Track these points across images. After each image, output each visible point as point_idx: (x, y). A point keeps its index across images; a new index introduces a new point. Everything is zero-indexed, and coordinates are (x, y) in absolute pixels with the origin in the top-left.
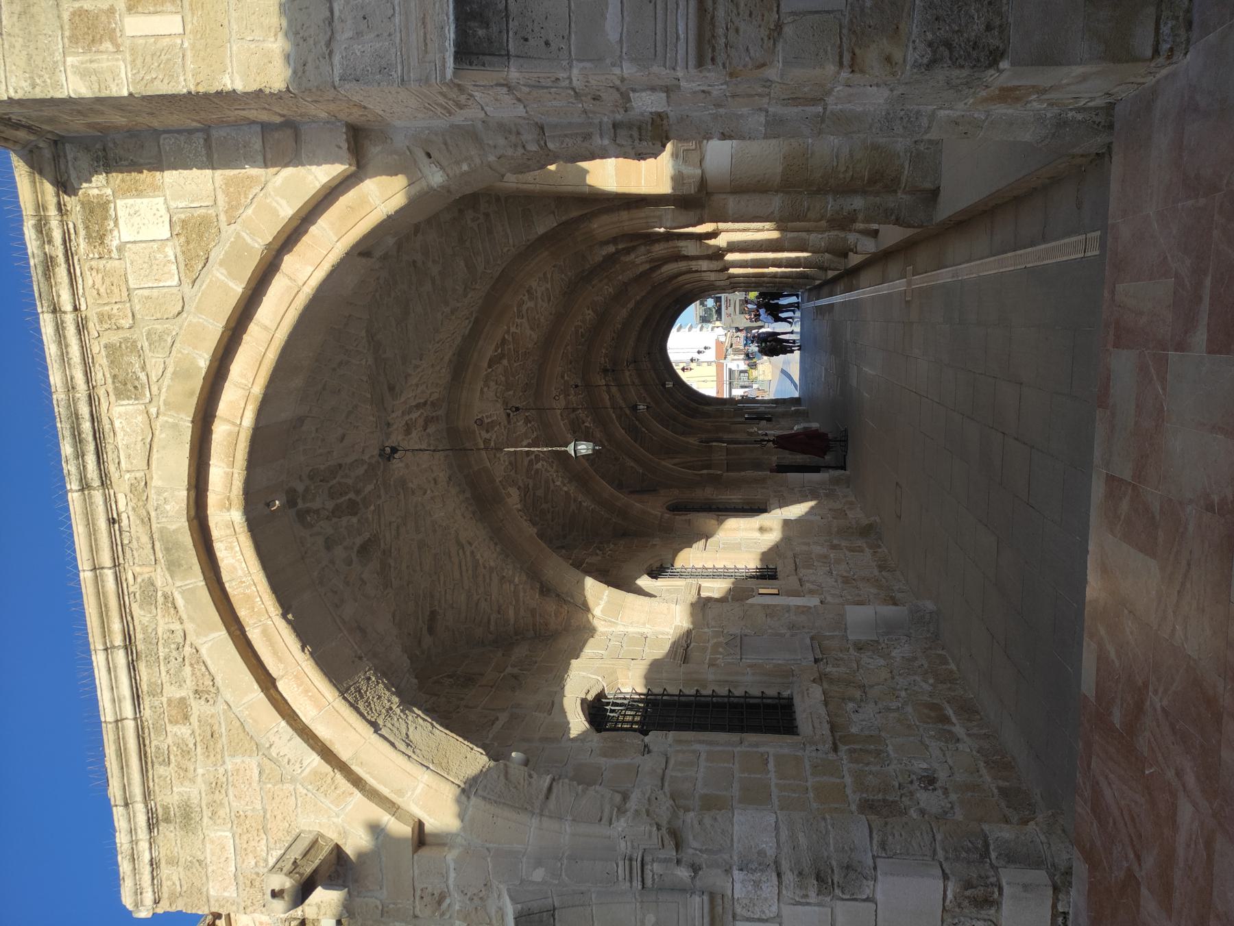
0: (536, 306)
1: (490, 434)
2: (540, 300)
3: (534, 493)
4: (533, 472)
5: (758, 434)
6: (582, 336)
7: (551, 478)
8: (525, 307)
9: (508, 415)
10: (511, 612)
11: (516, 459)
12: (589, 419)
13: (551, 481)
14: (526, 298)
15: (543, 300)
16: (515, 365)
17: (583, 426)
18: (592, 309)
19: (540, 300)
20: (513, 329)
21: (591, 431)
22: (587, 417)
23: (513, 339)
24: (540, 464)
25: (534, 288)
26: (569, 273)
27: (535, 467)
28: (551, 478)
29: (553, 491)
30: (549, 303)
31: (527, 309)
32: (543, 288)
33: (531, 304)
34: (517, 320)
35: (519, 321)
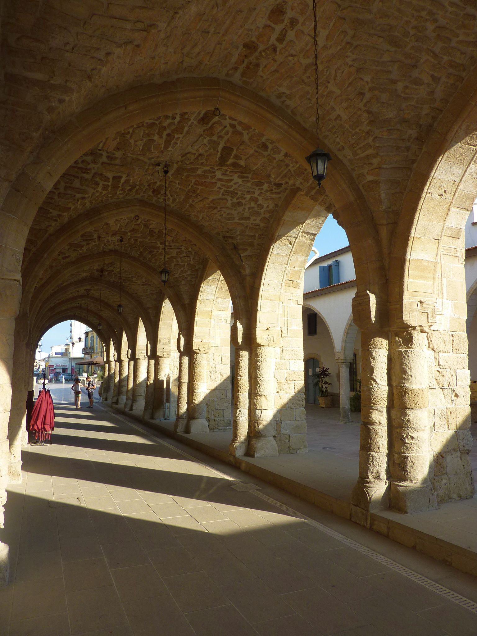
3: (77, 177)
4: (97, 179)
8: (229, 198)
9: (158, 165)
10: (38, 76)
11: (116, 165)
13: (84, 196)
14: (235, 200)
15: (228, 214)
16: (193, 181)
17: (84, 243)
19: (229, 211)
20: (219, 184)
21: (79, 249)
25: (239, 208)
26: (239, 238)
27: (101, 183)
28: (87, 196)
29: (75, 196)
30: (225, 218)
31: (227, 200)
33: (229, 204)
35: (222, 191)
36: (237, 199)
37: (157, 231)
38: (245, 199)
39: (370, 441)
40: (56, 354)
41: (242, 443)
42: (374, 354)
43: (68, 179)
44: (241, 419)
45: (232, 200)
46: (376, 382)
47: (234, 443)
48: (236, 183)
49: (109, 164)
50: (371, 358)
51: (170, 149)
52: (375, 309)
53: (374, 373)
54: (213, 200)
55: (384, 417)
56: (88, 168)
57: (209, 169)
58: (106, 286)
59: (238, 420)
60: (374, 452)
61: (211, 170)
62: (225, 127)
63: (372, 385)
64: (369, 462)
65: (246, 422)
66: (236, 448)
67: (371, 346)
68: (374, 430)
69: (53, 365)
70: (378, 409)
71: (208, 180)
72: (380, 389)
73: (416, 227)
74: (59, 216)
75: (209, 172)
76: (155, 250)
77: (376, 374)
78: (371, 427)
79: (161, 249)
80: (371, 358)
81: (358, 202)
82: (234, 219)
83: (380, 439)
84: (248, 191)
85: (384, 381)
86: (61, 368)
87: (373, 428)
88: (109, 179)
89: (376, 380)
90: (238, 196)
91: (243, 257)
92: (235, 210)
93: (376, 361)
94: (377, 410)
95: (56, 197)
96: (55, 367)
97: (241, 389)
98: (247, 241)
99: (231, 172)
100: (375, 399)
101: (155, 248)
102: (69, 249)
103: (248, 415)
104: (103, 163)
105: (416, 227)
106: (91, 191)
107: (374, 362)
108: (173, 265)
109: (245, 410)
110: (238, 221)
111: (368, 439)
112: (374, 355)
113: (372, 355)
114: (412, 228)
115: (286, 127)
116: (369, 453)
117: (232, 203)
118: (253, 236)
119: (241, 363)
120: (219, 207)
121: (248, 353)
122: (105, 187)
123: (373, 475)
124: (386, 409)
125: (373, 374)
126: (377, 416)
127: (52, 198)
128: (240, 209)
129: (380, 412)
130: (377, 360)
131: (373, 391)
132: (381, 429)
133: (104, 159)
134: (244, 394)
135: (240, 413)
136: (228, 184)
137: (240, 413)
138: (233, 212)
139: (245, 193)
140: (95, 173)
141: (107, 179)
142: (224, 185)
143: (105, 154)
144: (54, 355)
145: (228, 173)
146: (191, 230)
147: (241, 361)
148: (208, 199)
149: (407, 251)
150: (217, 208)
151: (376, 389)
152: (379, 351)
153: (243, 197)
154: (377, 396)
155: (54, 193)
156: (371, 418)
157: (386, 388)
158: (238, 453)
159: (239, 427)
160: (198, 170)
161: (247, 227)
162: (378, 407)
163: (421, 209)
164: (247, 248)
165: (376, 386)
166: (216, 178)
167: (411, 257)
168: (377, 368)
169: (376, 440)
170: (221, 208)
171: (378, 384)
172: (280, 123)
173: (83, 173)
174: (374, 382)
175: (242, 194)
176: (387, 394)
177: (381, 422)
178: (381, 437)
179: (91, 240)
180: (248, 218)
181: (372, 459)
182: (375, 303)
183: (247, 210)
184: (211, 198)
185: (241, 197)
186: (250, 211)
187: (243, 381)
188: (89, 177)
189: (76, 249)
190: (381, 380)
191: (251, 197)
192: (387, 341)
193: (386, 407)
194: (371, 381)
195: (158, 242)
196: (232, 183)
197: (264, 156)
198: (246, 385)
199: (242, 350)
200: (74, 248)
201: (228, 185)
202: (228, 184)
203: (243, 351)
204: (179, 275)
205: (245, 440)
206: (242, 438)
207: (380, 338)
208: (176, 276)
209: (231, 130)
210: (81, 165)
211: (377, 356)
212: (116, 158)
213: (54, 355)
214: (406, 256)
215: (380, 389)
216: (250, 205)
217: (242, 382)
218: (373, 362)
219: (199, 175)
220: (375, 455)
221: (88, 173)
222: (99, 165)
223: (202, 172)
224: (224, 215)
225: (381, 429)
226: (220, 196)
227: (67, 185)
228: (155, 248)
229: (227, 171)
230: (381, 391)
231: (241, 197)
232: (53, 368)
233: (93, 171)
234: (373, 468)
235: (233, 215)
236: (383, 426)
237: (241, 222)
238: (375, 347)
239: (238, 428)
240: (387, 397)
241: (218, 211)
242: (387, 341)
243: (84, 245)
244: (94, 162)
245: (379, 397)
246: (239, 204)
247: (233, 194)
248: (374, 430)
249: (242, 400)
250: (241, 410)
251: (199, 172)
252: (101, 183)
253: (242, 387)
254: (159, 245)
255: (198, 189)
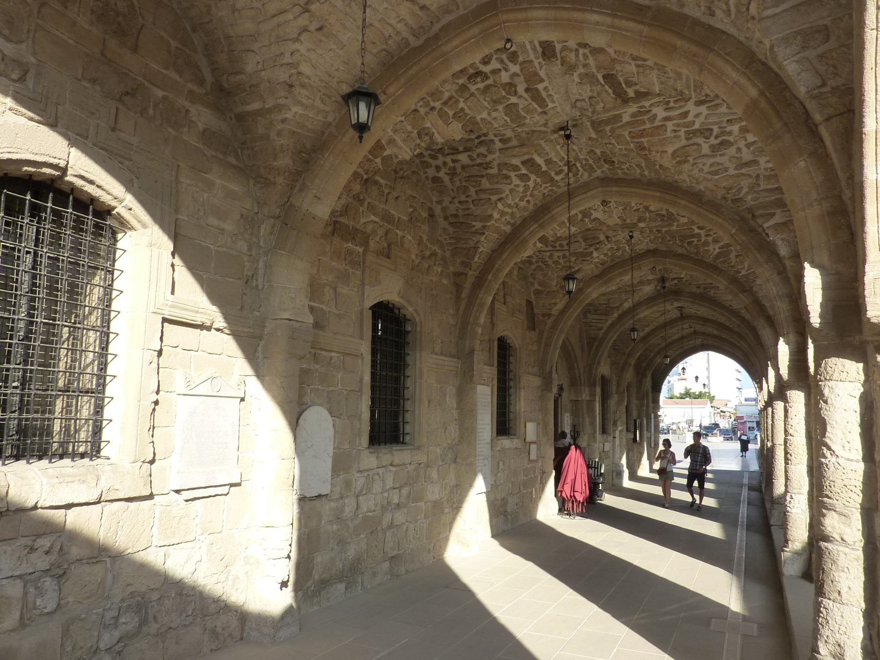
0: (703, 156)
1: (525, 95)
2: (712, 160)
3: (482, 176)
4: (505, 172)
5: (614, 431)
6: (690, 243)
7: (503, 195)
8: (700, 140)
12: (602, 257)
14: (713, 141)
15: (711, 165)
16: (626, 133)
17: (592, 249)
18: (719, 253)
19: (712, 160)
20: (670, 125)
21: (588, 259)
22: (606, 255)
23: (658, 127)
24: (518, 182)
26: (749, 197)
27: (512, 174)
28: (503, 195)
29: (490, 199)
30: (710, 173)
32: (727, 164)
33: (706, 149)
34: (683, 130)
35: (682, 133)
36: (716, 137)
37: (664, 212)
38: (730, 133)
39: (823, 575)
40: (746, 400)
41: (796, 553)
42: (826, 392)
43: (473, 181)
44: (793, 511)
45: (708, 143)
46: (832, 453)
47: (783, 551)
48: (697, 116)
49: (507, 149)
50: (821, 401)
51: (551, 105)
52: (819, 299)
53: (827, 433)
54: (675, 152)
55: (854, 529)
56: (488, 161)
57: (637, 110)
58: (690, 299)
59: (788, 512)
60: (830, 599)
61: (641, 110)
62: (577, 50)
63: (826, 458)
64: (821, 619)
65: (803, 517)
66: (785, 561)
67: (821, 375)
68: (829, 554)
69: (743, 417)
70: (837, 509)
71: (648, 126)
72: (839, 467)
73: (876, 108)
74: (484, 227)
75: (640, 113)
76: (695, 240)
77: (830, 435)
78: (823, 544)
79: (703, 235)
80: (821, 401)
81: (768, 94)
82: (726, 169)
83: (842, 574)
84: (728, 120)
85: (854, 451)
86: (755, 420)
87: (827, 549)
88: (517, 166)
89: (832, 448)
90: (715, 133)
91: (768, 228)
92: (721, 155)
93: (831, 407)
94: (835, 511)
95: (472, 206)
96: (745, 420)
97: (793, 457)
98: (767, 199)
99: (675, 102)
100: (830, 486)
101: (693, 236)
102: (575, 260)
103: (809, 505)
104: (500, 150)
105: (876, 108)
106: (507, 188)
107: (828, 409)
108: (733, 256)
109: (802, 496)
110: (737, 172)
111: (819, 569)
112: (826, 395)
113: (823, 395)
114: (865, 114)
115: (608, 20)
116: (820, 599)
117: (710, 147)
118: (776, 189)
119: (789, 412)
120: (690, 159)
121: (803, 394)
122: (524, 178)
123: (830, 648)
124: (859, 510)
125: (826, 434)
126: (836, 524)
127: (468, 209)
128: (732, 151)
129: (843, 517)
130: (832, 404)
131: (826, 469)
132: (846, 554)
133: (498, 145)
134: (799, 467)
135: (792, 500)
136: (685, 121)
137: (792, 500)
138: (718, 159)
139: (724, 125)
140: (499, 165)
141: (516, 168)
142: (678, 125)
143: (496, 140)
144: (744, 402)
145: (672, 104)
146: (683, 202)
147: (790, 409)
148: (666, 152)
149: (863, 165)
150: (688, 161)
151: (831, 466)
152: (836, 386)
153: (725, 131)
154: (834, 482)
155: (467, 202)
156: (823, 526)
157: (861, 467)
158: (788, 571)
159: (790, 525)
160: (621, 117)
161: (758, 176)
162: (836, 506)
163: (876, 67)
164: (773, 211)
165: (833, 459)
166: (659, 118)
167: (879, 175)
168: (834, 423)
169: (833, 574)
170: (694, 159)
171: (837, 456)
172: (596, 17)
173: (487, 169)
174: (828, 452)
175: (720, 128)
176: (861, 479)
177: (845, 538)
178: (846, 570)
179: (598, 243)
180: (755, 162)
181: (825, 613)
182: (821, 287)
183: (745, 150)
184: (670, 150)
185: (722, 133)
186: (752, 149)
187: (795, 443)
188: (494, 171)
189: (584, 259)
190: (843, 447)
191: (740, 127)
192: (861, 365)
193: (859, 506)
194: (823, 450)
195: (694, 227)
196: (690, 117)
197: (651, 68)
198: (801, 452)
199: (790, 389)
200: (581, 259)
201: (685, 123)
202: (685, 121)
203: (794, 391)
204: (747, 270)
205: (803, 549)
206: (796, 546)
207: (838, 357)
208: (743, 272)
209: (587, 51)
210: (479, 161)
211: (833, 397)
212: (509, 139)
213: (744, 402)
214: (863, 176)
215: (839, 467)
216: (746, 140)
217: (793, 446)
218: (826, 409)
219: (628, 123)
220: (832, 607)
221: (491, 168)
222: (498, 154)
223: (632, 117)
224: (706, 169)
225: (846, 554)
226: (684, 142)
227: (477, 188)
228: (693, 236)
229: (668, 103)
230: (844, 471)
231: (722, 133)
232: (743, 421)
233: (495, 163)
234: (828, 633)
235: (722, 164)
236: (851, 547)
237: (744, 171)
238: (828, 378)
239: (789, 527)
240: (861, 485)
241: (693, 166)
242: (861, 365)
243: (592, 252)
244: (490, 152)
245: (839, 483)
246: (725, 144)
247: (706, 132)
248: (829, 554)
249: (794, 478)
250: (793, 495)
251: (626, 118)
252: (512, 174)
253: (792, 454)
254: (697, 231)
255: (642, 142)
